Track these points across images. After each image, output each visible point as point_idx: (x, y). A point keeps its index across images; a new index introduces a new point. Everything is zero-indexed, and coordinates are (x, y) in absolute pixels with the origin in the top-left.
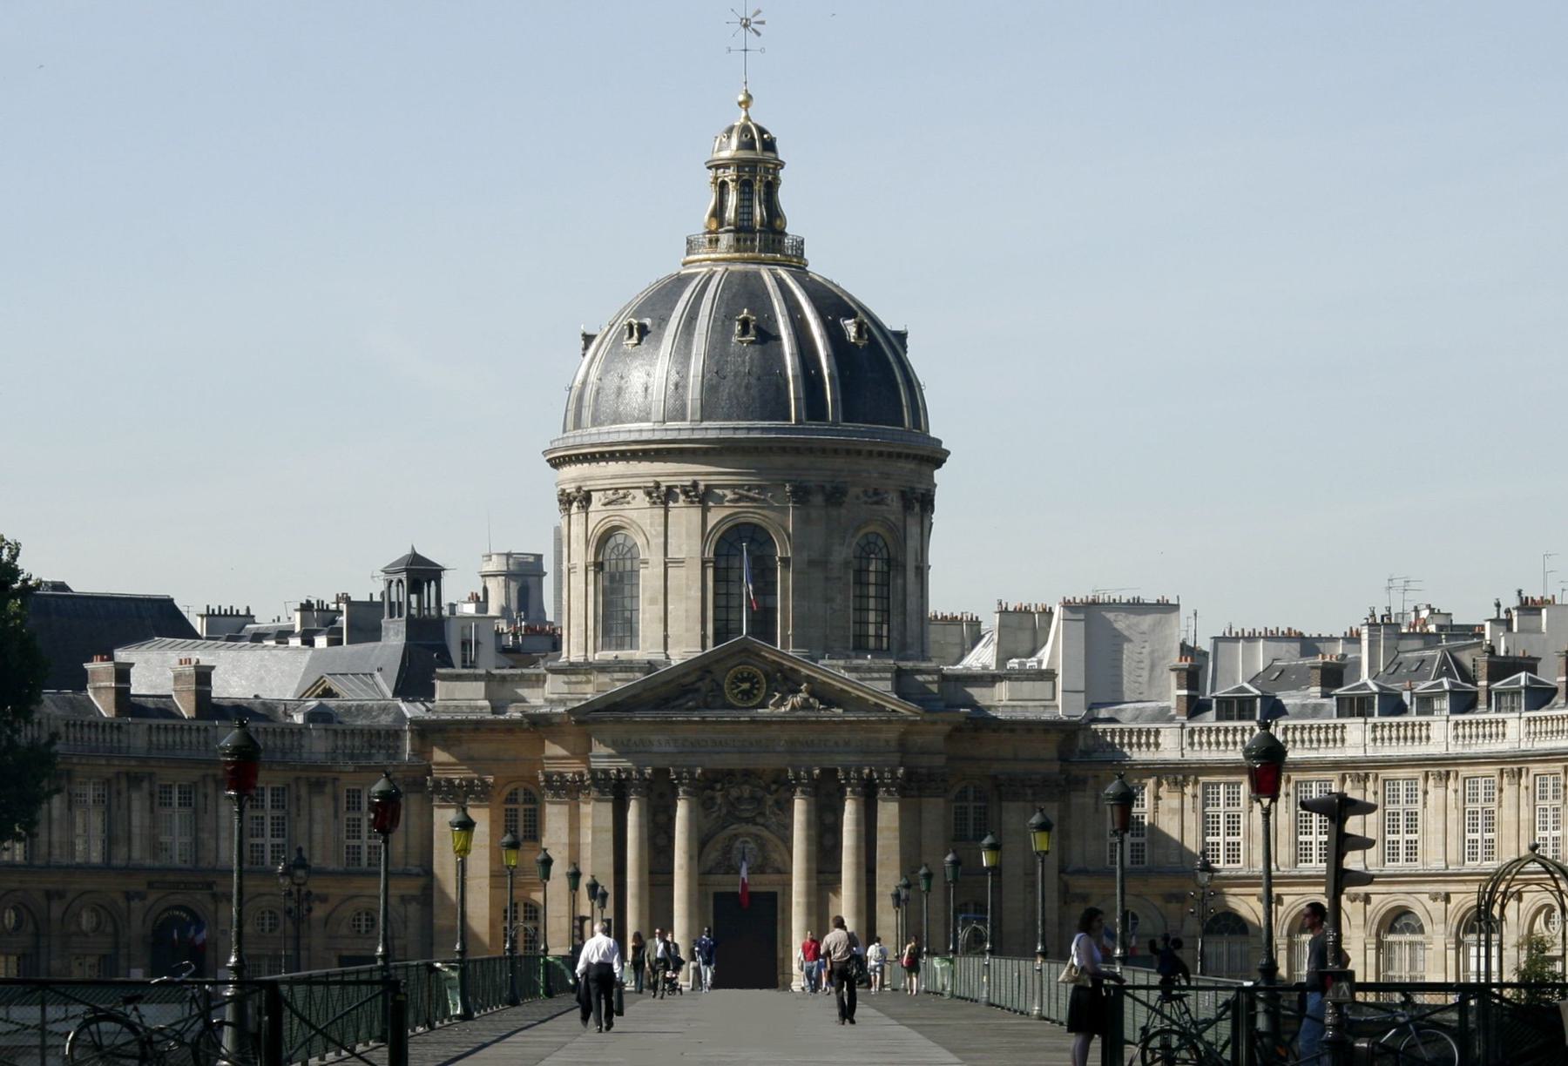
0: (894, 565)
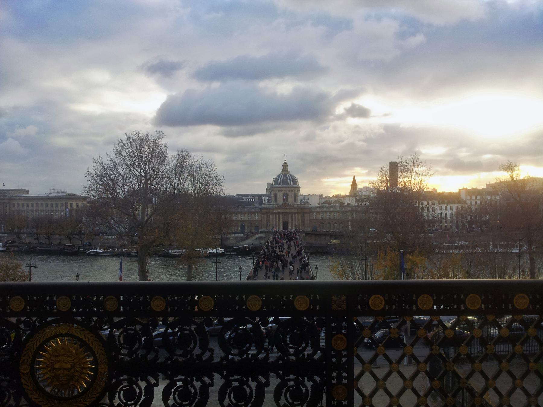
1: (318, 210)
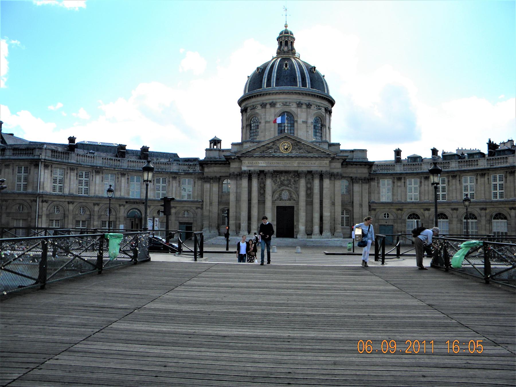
0: (323, 125)
1: (399, 169)
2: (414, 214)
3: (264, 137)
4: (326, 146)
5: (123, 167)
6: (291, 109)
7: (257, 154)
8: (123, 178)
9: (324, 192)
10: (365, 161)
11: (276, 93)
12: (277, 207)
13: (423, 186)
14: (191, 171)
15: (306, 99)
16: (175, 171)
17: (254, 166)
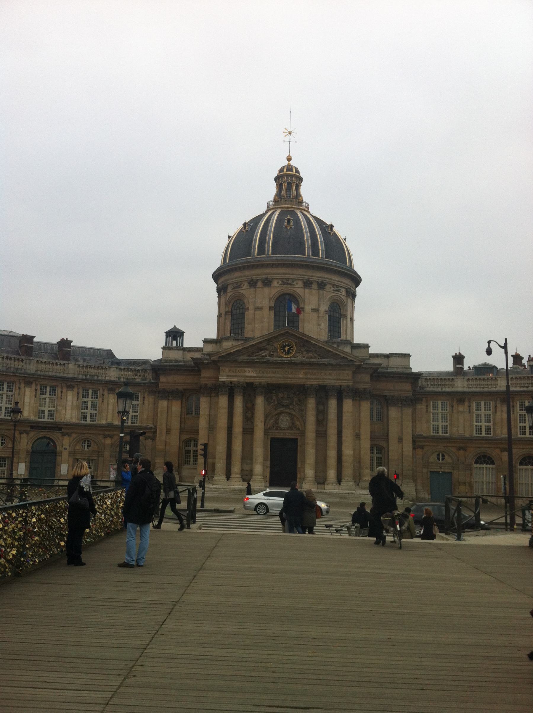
1: (460, 385)
2: (484, 456)
3: (253, 331)
4: (348, 349)
5: (28, 371)
6: (295, 289)
7: (241, 358)
8: (28, 390)
9: (344, 418)
10: (407, 371)
11: (273, 266)
12: (271, 438)
13: (499, 413)
14: (139, 380)
15: (317, 276)
16: (113, 379)
17: (240, 376)
